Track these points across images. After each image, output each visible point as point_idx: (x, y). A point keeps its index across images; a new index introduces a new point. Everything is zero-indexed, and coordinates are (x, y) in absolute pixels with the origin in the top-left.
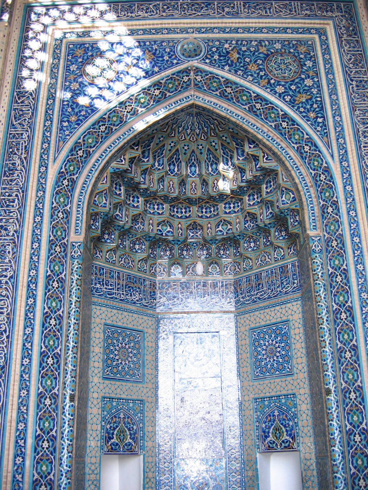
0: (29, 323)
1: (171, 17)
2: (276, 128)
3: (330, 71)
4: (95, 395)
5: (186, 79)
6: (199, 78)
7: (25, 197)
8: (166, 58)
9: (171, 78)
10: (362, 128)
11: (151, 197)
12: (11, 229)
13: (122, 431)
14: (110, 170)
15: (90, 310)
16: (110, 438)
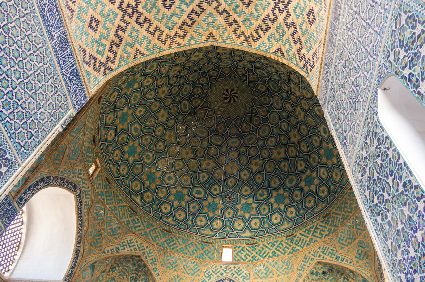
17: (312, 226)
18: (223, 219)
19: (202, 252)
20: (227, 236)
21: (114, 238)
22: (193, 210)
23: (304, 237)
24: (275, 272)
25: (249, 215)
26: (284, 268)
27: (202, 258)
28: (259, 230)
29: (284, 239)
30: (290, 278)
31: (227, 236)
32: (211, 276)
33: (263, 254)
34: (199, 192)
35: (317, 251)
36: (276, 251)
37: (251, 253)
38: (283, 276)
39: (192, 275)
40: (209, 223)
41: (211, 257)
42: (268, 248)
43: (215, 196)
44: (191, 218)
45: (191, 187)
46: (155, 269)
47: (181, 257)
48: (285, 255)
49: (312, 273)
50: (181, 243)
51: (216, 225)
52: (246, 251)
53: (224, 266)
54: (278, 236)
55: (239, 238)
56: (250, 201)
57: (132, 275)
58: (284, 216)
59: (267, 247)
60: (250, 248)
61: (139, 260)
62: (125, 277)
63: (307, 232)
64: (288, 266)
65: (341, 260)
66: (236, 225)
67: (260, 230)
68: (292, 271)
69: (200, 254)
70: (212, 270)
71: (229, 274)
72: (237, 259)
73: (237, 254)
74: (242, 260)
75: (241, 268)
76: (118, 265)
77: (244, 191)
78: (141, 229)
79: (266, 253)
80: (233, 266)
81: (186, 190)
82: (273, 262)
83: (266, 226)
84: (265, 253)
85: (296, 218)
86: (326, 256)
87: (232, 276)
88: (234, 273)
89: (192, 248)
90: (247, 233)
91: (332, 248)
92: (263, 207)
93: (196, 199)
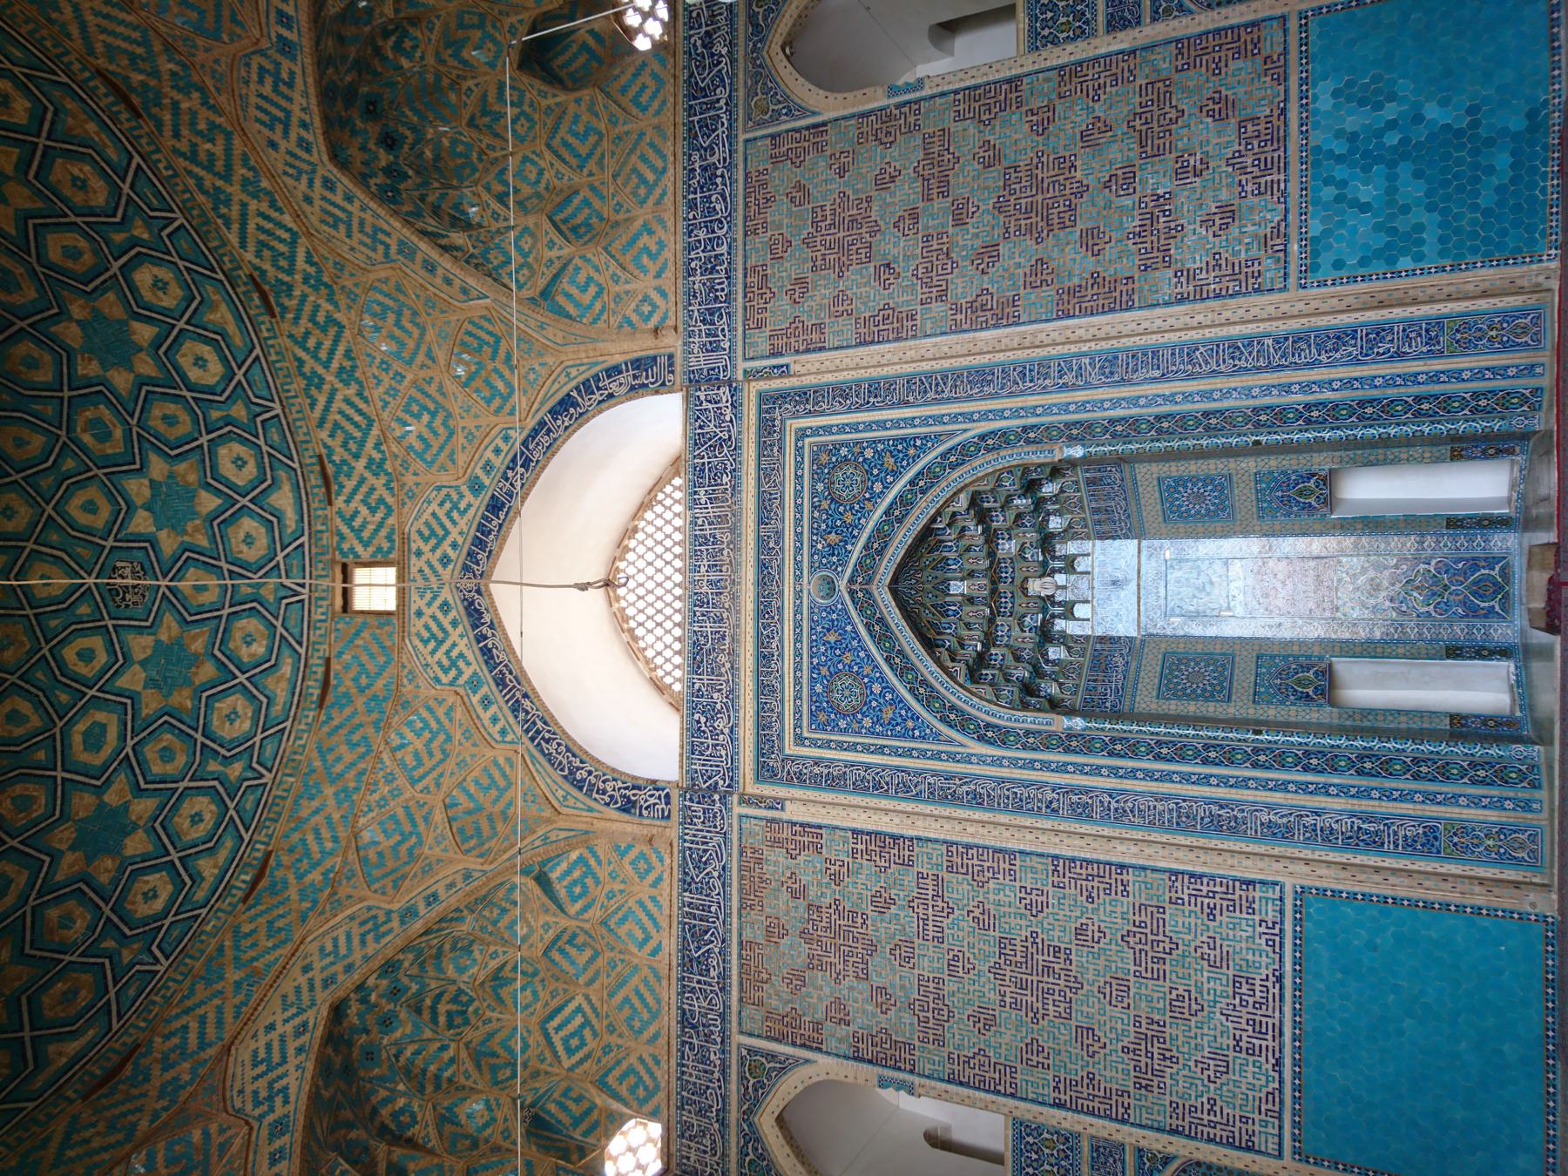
0: (1166, 777)
1: (780, 610)
2: (923, 492)
3: (854, 428)
4: (1251, 711)
5: (860, 595)
6: (860, 579)
7: (1011, 780)
8: (834, 616)
9: (861, 611)
10: (931, 395)
11: (990, 640)
12: (1050, 795)
13: (1299, 682)
14: (968, 685)
15: (1141, 714)
16: (1308, 695)
17: (191, 182)
18: (225, 612)
19: (360, 702)
20: (297, 594)
21: (221, 1158)
22: (181, 760)
23: (251, 227)
24: (422, 374)
25: (204, 494)
26: (397, 332)
27: (385, 699)
28: (265, 448)
29: (285, 326)
30: (428, 299)
31: (297, 594)
32: (454, 654)
33: (357, 425)
34: (94, 738)
35: (288, 158)
36: (335, 365)
37: (362, 481)
38: (431, 335)
39: (449, 739)
40: (242, 678)
41: (382, 660)
42: (330, 401)
43: (120, 659)
44: (213, 766)
45: (60, 774)
46: (409, 913)
47: (376, 796)
48: (345, 322)
49: (389, 196)
50: (315, 804)
51: (254, 646)
52: (353, 505)
53: (417, 602)
54: (273, 358)
55: (305, 539)
56: (137, 488)
57: (442, 1019)
58: (181, 324)
59: (327, 409)
60: (342, 486)
61: (364, 1000)
62: (447, 1055)
63: (224, 210)
64: (386, 308)
65: (289, 28)
66: (251, 554)
67: (261, 442)
68: (399, 288)
69: (370, 711)
70: (433, 653)
71: (446, 574)
72: (386, 545)
73: (366, 545)
74: (391, 521)
75: (420, 525)
76: (386, 1101)
77: (91, 517)
78: (219, 1010)
79: (350, 412)
80: (414, 559)
81: (75, 800)
82: (379, 382)
83: (243, 413)
84: (349, 419)
85: (181, 263)
86: (297, 113)
87: (449, 561)
88: (439, 553)
89: (343, 748)
90: (283, 499)
91: (255, 77)
92: (162, 428)
93: (129, 749)
